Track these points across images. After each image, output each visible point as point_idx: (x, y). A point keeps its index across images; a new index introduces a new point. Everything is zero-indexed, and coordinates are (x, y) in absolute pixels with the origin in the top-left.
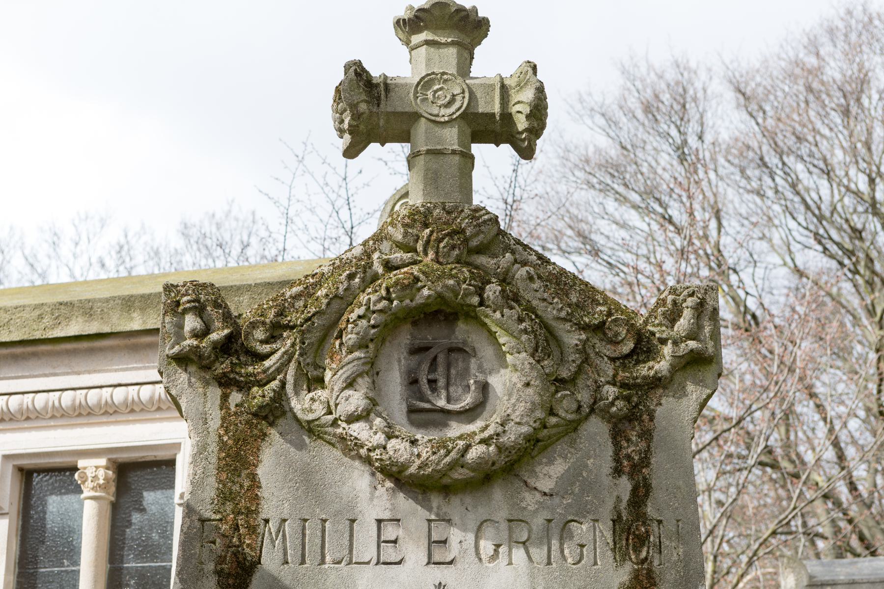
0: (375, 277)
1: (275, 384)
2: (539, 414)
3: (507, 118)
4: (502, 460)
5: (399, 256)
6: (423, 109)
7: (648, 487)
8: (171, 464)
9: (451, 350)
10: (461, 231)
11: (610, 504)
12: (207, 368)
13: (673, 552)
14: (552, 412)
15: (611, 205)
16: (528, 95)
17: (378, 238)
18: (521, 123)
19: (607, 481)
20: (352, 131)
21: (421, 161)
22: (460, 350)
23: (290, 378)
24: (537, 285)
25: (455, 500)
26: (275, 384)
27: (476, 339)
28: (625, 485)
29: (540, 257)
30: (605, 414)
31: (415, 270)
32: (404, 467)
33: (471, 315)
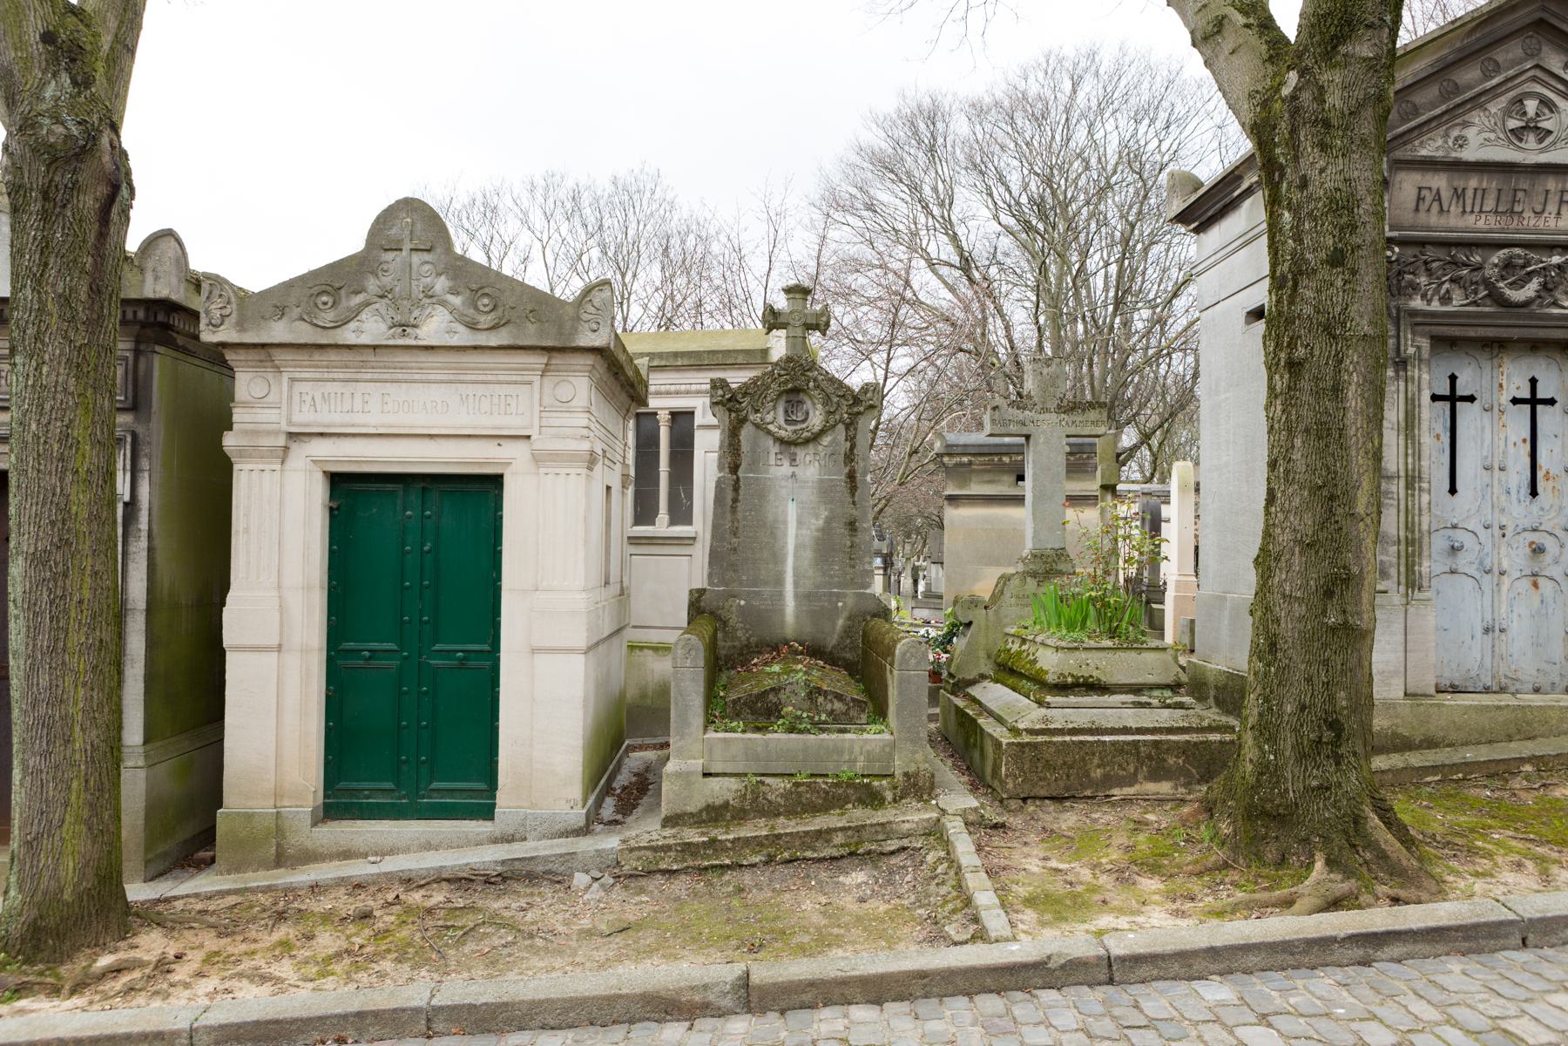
5: (782, 372)
6: (791, 322)
8: (693, 413)
13: (861, 464)
16: (824, 319)
27: (806, 399)
28: (848, 444)
30: (843, 423)
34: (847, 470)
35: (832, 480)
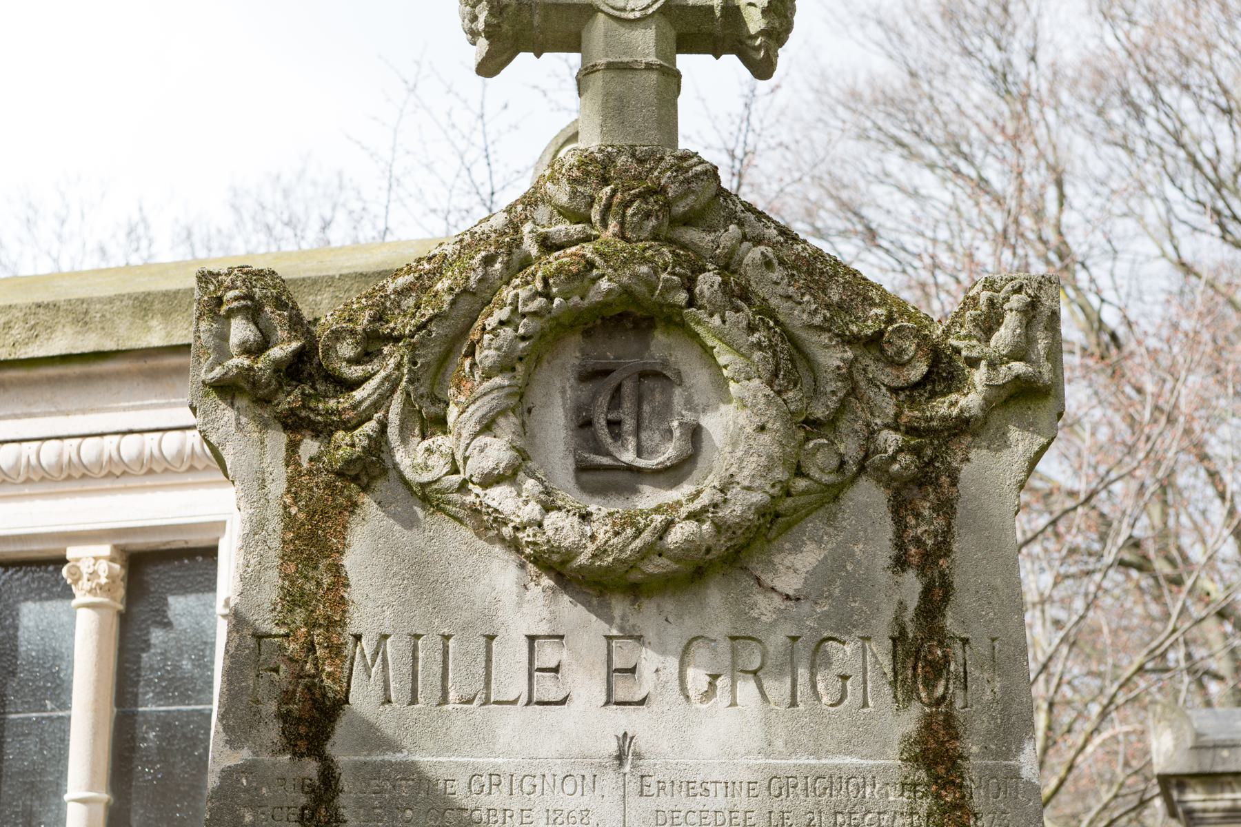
0: (526, 262)
1: (370, 427)
2: (780, 474)
3: (733, 13)
4: (723, 544)
5: (562, 228)
7: (947, 588)
8: (210, 553)
9: (644, 375)
10: (661, 190)
11: (888, 613)
12: (264, 401)
14: (799, 472)
15: (894, 162)
17: (531, 200)
18: (755, 22)
19: (884, 578)
20: (491, 33)
21: (598, 80)
22: (658, 375)
23: (394, 418)
24: (778, 273)
25: (649, 607)
26: (370, 427)
27: (683, 358)
28: (912, 585)
29: (784, 231)
30: (883, 475)
31: (588, 250)
32: (570, 554)
33: (675, 322)
34: (908, 722)
35: (831, 780)
